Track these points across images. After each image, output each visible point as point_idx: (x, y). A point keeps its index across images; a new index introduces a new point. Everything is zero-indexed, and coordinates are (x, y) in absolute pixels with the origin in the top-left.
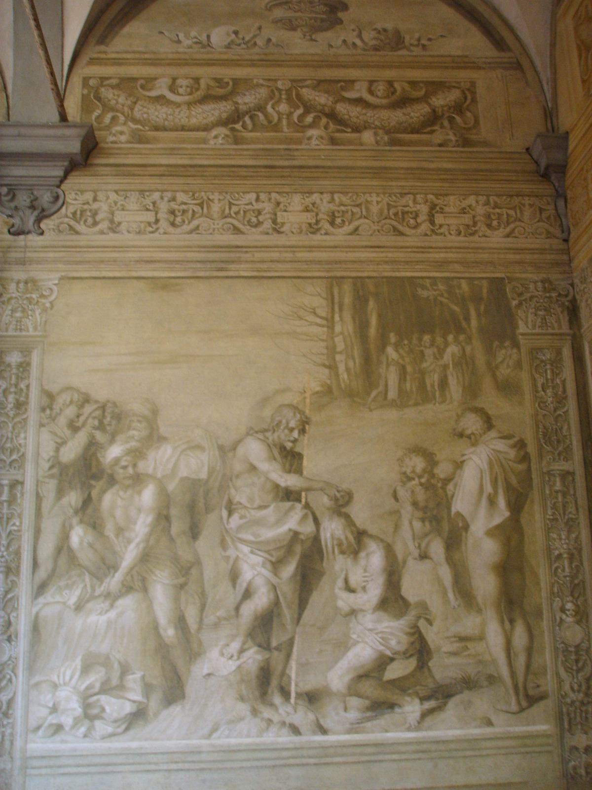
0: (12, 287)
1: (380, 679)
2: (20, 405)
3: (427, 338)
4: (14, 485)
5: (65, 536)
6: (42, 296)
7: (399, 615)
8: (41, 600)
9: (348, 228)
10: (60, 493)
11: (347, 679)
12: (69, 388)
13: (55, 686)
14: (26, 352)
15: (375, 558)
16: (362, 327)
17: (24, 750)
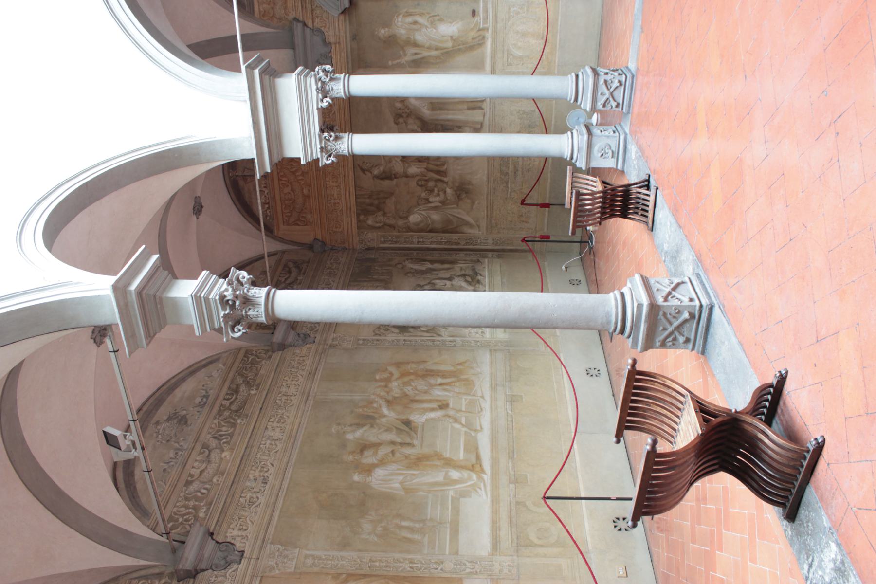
0: (334, 343)
1: (471, 282)
2: (378, 340)
3: (372, 271)
4: (405, 340)
5: (424, 331)
6: (339, 337)
7: (454, 278)
8: (443, 335)
9: (332, 282)
10: (410, 332)
11: (471, 286)
12: (374, 331)
13: (470, 333)
14: (359, 340)
15: (437, 281)
16: (366, 281)
17: (489, 338)
